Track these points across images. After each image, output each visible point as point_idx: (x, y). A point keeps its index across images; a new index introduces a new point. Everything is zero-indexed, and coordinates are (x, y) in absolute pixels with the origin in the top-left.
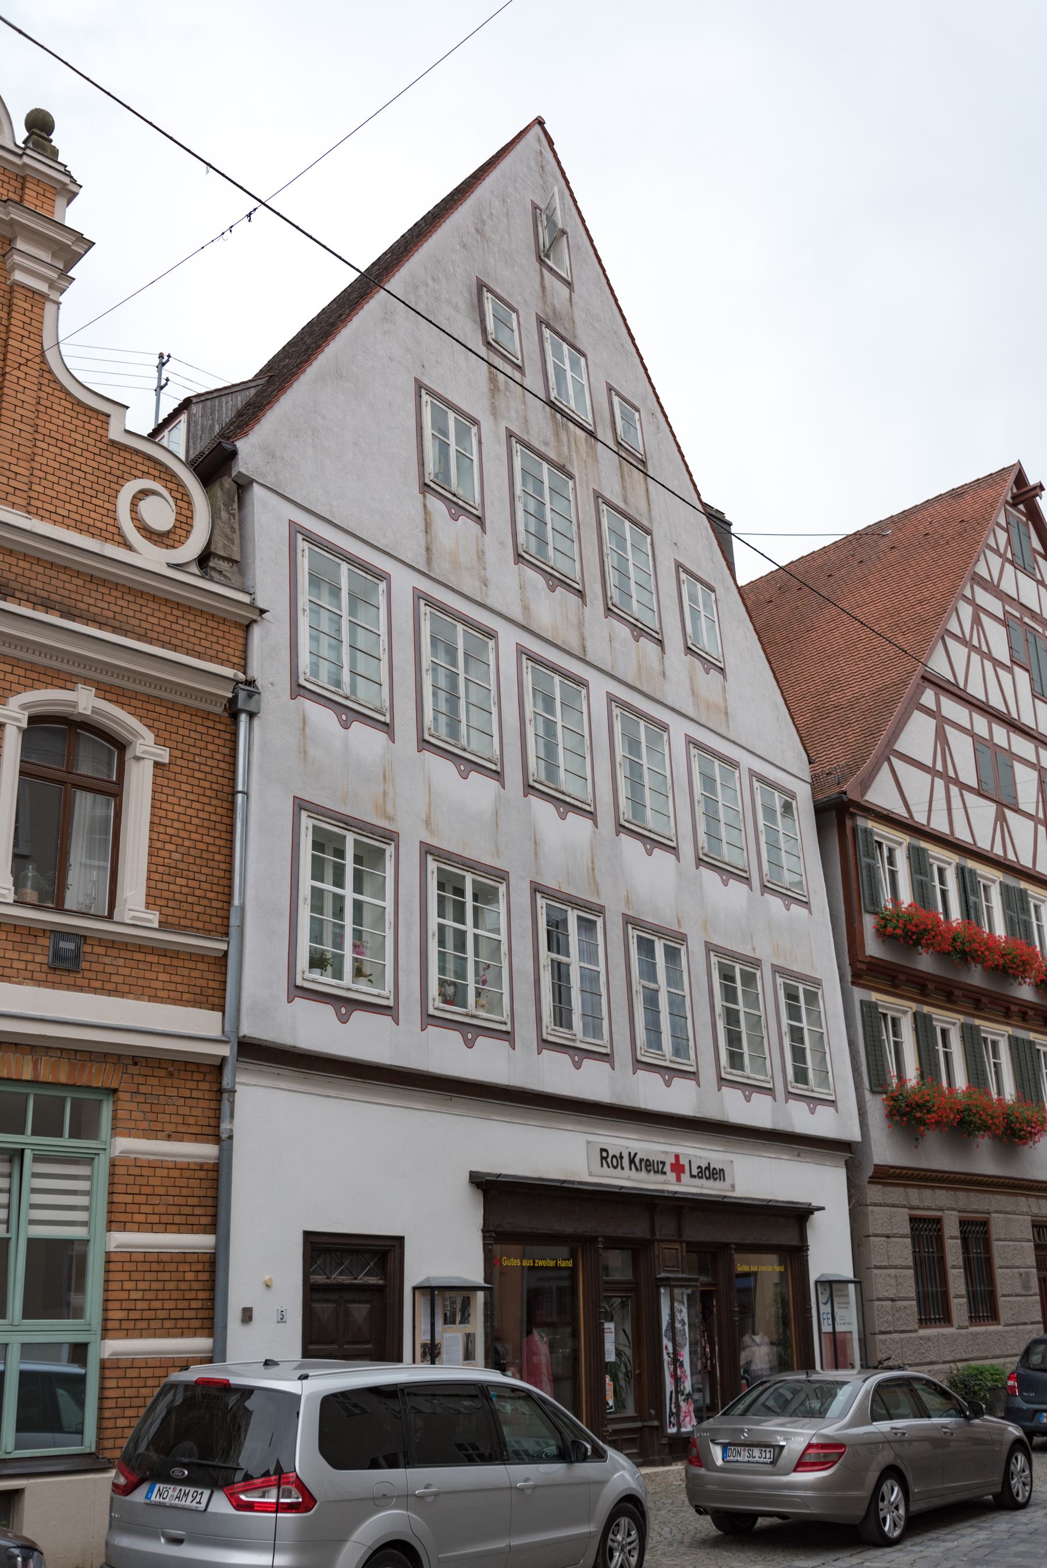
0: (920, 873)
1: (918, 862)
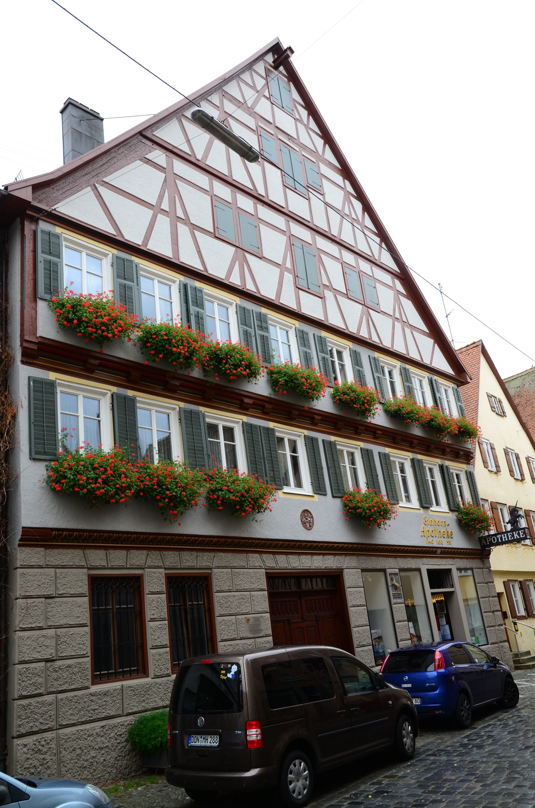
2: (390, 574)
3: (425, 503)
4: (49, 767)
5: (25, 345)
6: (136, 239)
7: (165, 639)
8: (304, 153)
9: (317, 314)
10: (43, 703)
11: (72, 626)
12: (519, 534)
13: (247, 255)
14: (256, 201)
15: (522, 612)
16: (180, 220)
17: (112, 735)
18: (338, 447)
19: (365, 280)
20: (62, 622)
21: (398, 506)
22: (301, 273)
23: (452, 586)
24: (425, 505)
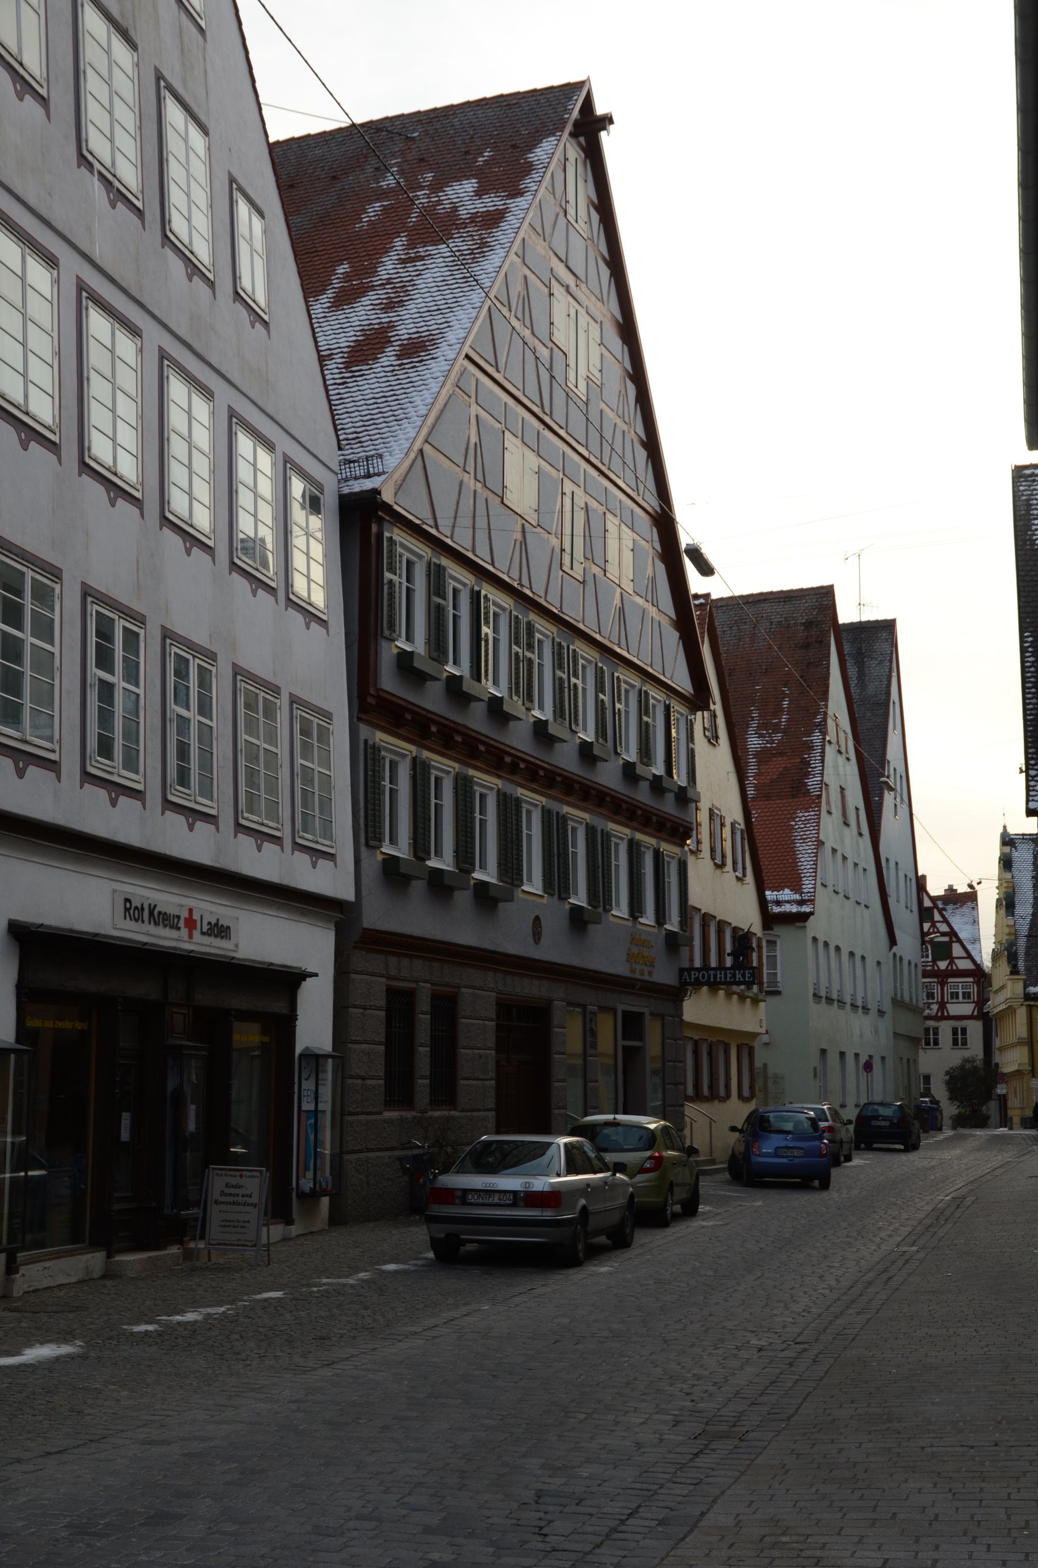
0: (438, 595)
1: (436, 578)
23: (641, 1039)
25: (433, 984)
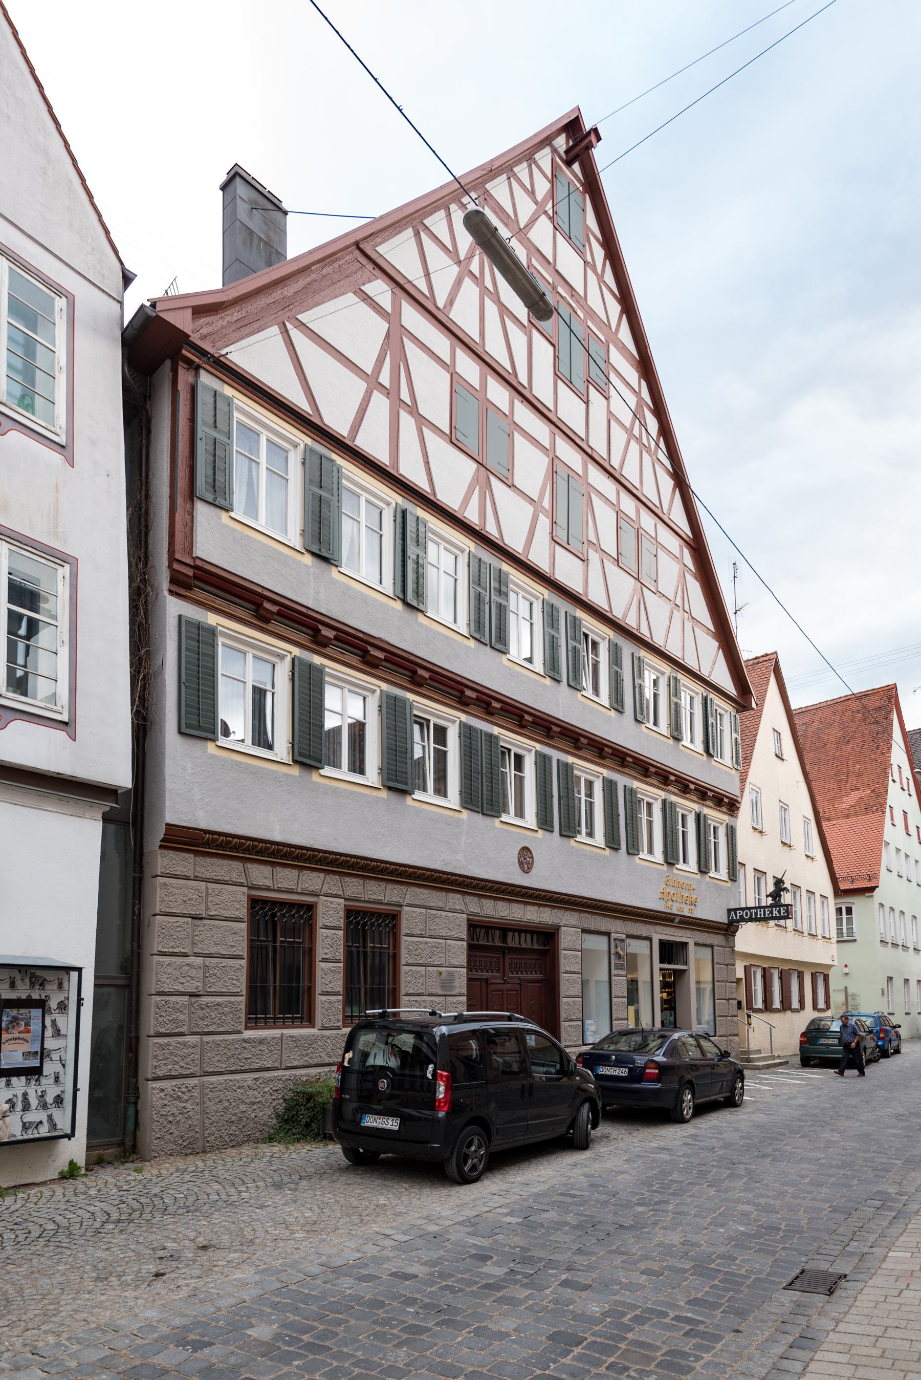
2: (615, 940)
3: (670, 859)
4: (190, 1117)
5: (176, 566)
6: (340, 425)
7: (338, 984)
8: (590, 324)
9: (574, 584)
10: (185, 1044)
11: (223, 957)
12: (779, 912)
13: (492, 478)
14: (514, 393)
15: (759, 1004)
16: (403, 405)
17: (267, 1089)
18: (576, 772)
19: (645, 543)
20: (213, 950)
21: (637, 857)
22: (561, 519)
23: (686, 963)
24: (670, 861)
25: (346, 899)
